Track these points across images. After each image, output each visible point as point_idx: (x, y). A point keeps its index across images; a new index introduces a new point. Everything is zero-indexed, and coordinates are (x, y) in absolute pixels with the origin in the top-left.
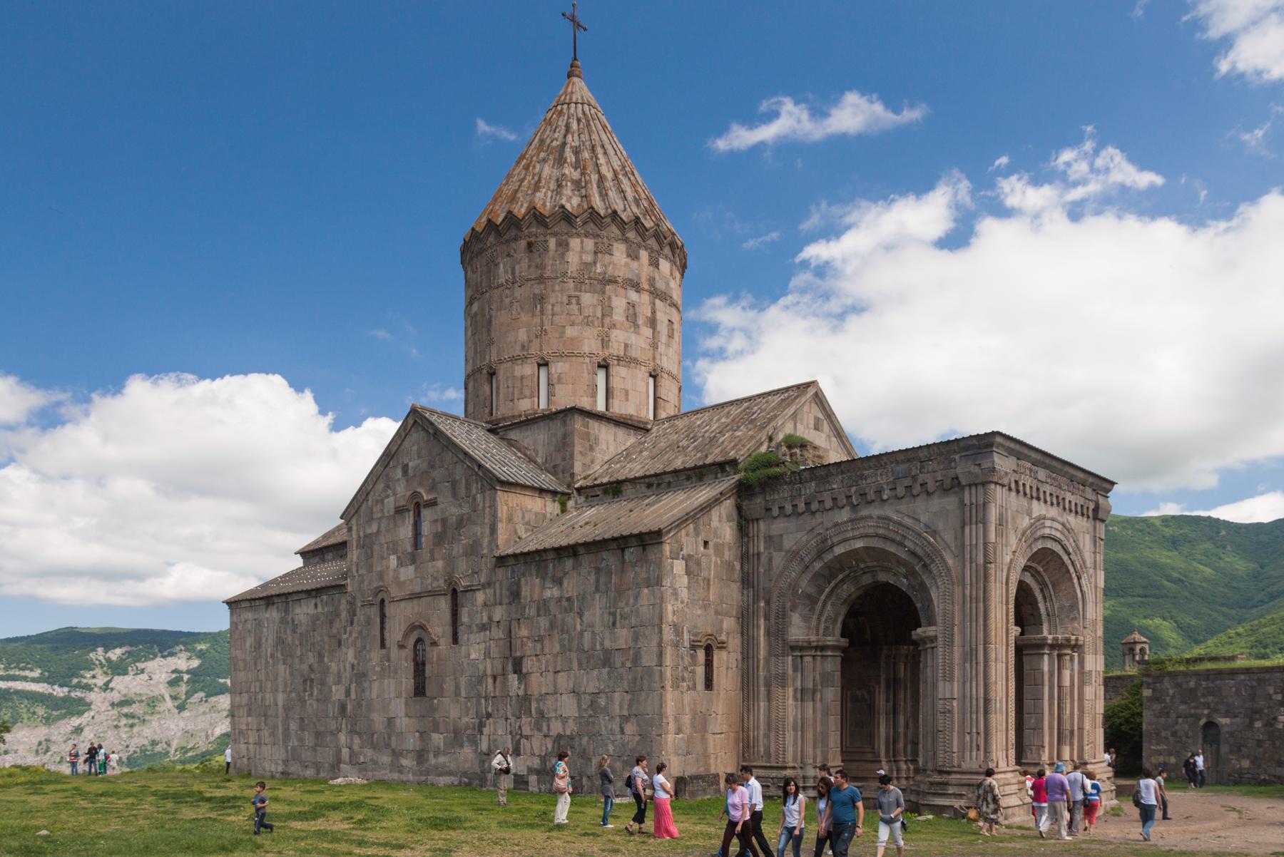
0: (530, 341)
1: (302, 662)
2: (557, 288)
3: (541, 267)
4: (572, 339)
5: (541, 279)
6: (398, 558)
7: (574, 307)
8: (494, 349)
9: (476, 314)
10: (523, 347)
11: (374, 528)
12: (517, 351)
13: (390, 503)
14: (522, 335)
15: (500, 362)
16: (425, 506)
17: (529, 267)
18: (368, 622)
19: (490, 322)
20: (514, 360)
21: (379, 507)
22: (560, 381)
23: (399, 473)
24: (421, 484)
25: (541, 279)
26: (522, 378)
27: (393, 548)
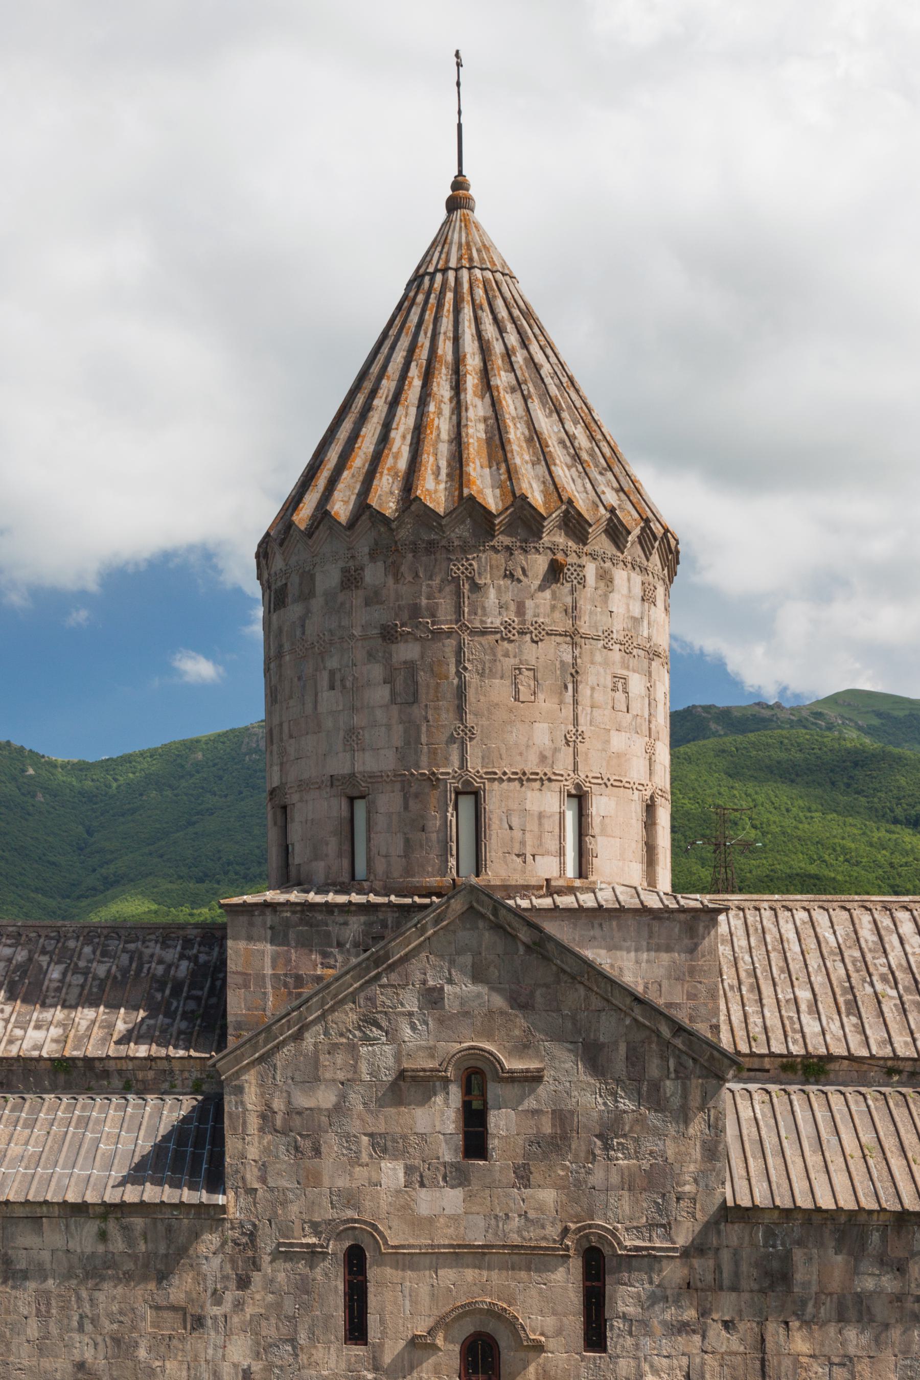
0: (556, 750)
1: (42, 1348)
2: (598, 658)
3: (572, 612)
4: (619, 755)
5: (573, 637)
6: (409, 1170)
7: (620, 695)
8: (474, 752)
9: (411, 668)
10: (543, 758)
11: (325, 1098)
12: (531, 765)
13: (379, 1058)
14: (542, 735)
15: (493, 778)
16: (501, 1080)
17: (553, 608)
18: (304, 1287)
19: (461, 693)
20: (522, 778)
21: (340, 1059)
22: (604, 832)
23: (411, 1002)
24: (489, 1035)
25: (573, 637)
26: (541, 816)
27: (383, 1146)
